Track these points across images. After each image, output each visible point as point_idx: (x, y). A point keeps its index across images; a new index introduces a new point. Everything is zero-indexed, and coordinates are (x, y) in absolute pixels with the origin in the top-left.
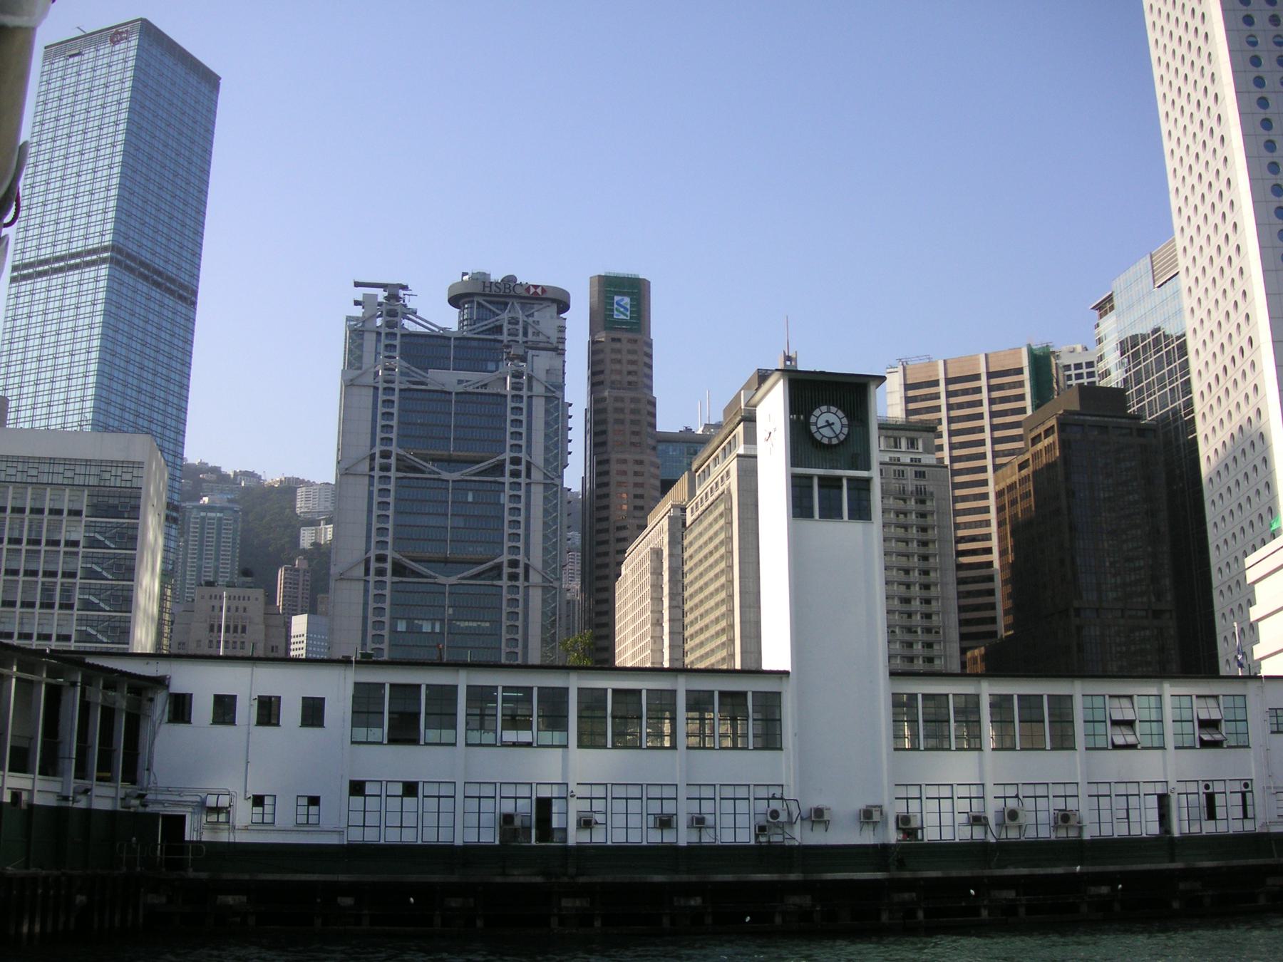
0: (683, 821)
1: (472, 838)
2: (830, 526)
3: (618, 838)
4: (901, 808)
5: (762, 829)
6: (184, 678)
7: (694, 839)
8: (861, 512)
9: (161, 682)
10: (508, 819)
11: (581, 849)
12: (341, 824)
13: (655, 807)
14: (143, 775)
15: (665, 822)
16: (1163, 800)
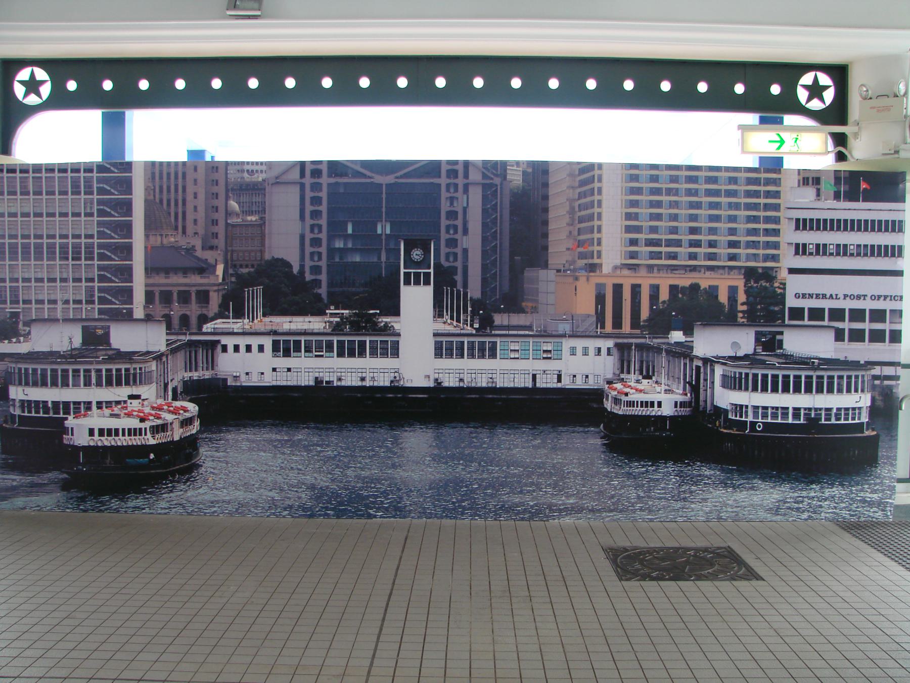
0: (368, 379)
1: (307, 384)
2: (417, 288)
3: (349, 384)
4: (436, 376)
5: (392, 382)
6: (225, 340)
7: (371, 384)
8: (427, 283)
9: (219, 341)
10: (316, 378)
11: (338, 387)
12: (269, 380)
13: (360, 375)
14: (216, 368)
15: (363, 379)
16: (534, 376)
